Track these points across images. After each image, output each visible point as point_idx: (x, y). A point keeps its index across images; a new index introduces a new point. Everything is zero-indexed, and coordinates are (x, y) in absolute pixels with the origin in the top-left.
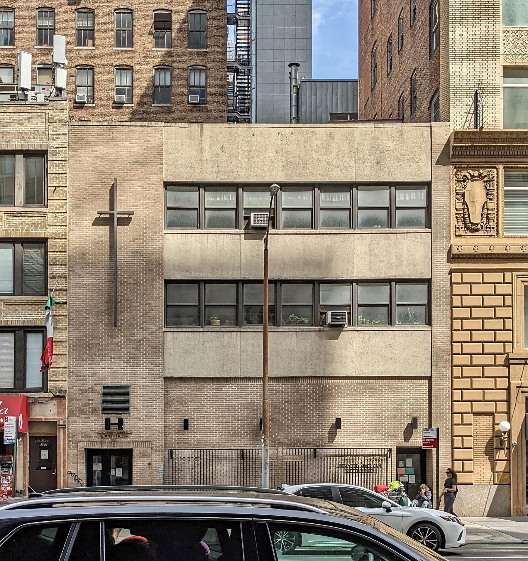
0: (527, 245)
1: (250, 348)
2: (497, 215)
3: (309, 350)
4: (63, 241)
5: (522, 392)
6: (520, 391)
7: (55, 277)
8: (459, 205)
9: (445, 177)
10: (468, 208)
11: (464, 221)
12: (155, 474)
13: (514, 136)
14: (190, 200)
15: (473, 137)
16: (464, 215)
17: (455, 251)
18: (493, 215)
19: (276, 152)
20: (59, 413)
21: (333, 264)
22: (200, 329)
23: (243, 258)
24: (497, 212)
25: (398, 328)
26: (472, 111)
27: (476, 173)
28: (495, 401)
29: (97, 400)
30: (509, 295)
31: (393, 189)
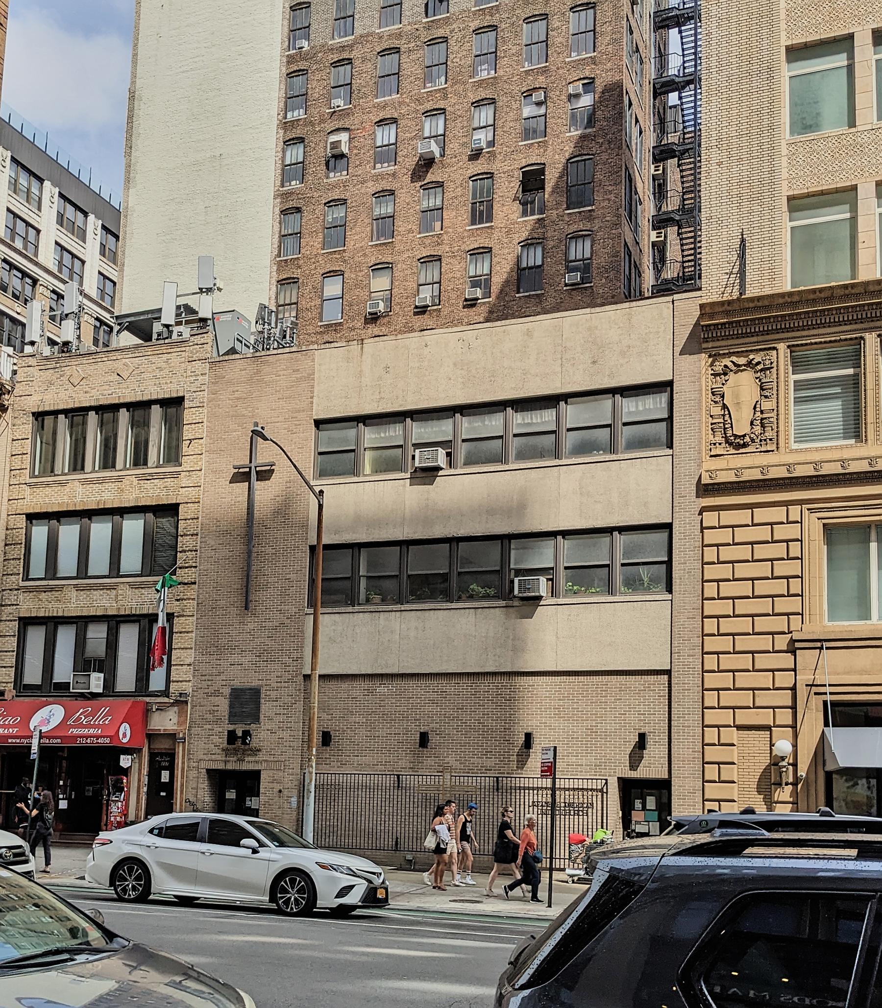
0: (879, 457)
1: (412, 634)
2: (777, 420)
3: (491, 634)
4: (196, 505)
5: (816, 694)
6: (812, 692)
7: (185, 551)
8: (717, 410)
9: (694, 374)
10: (729, 414)
11: (725, 433)
12: (286, 805)
13: (796, 298)
15: (730, 308)
16: (723, 425)
17: (706, 480)
18: (771, 420)
19: (455, 364)
20: (179, 723)
21: (528, 510)
22: (350, 609)
23: (407, 511)
24: (778, 415)
25: (622, 599)
26: (736, 270)
27: (742, 361)
28: (773, 708)
29: (223, 705)
30: (797, 540)
31: (618, 396)
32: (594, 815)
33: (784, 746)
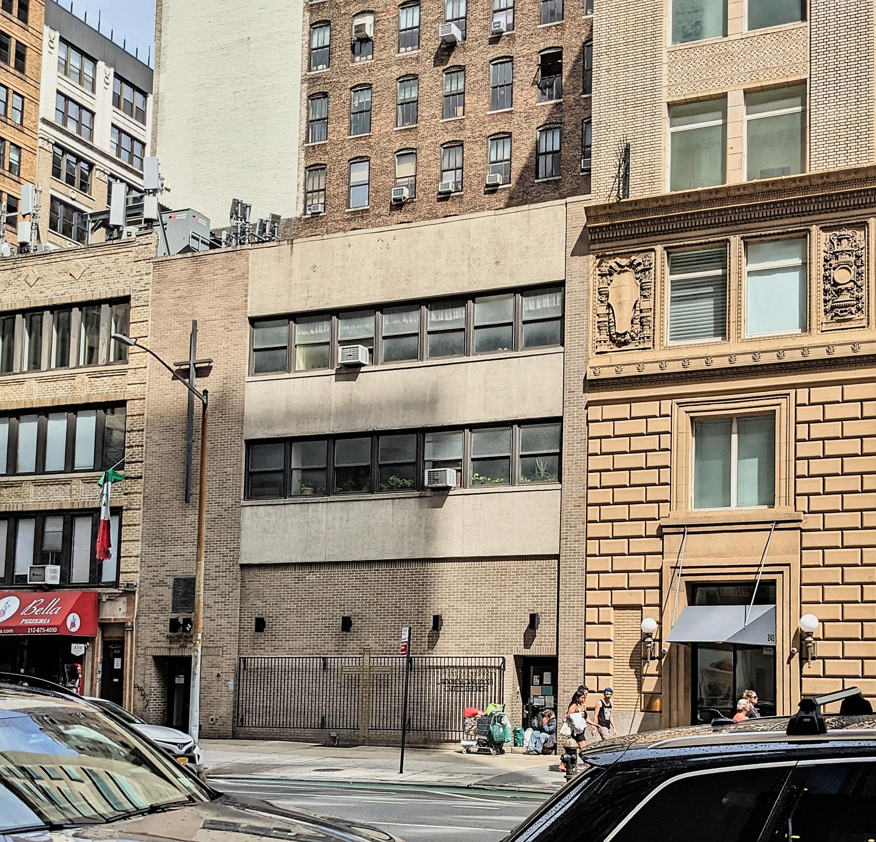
1: (337, 524)
3: (406, 523)
4: (142, 401)
7: (132, 447)
8: (603, 310)
9: (583, 273)
12: (224, 688)
14: (274, 339)
16: (606, 324)
18: (649, 318)
19: (375, 264)
20: (128, 612)
22: (282, 501)
23: (333, 406)
27: (624, 262)
29: (167, 594)
31: (518, 296)
32: (492, 691)
33: (650, 624)
